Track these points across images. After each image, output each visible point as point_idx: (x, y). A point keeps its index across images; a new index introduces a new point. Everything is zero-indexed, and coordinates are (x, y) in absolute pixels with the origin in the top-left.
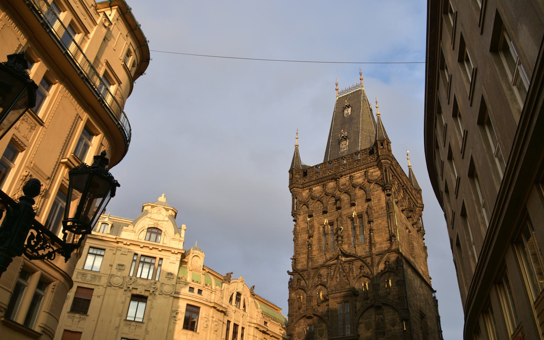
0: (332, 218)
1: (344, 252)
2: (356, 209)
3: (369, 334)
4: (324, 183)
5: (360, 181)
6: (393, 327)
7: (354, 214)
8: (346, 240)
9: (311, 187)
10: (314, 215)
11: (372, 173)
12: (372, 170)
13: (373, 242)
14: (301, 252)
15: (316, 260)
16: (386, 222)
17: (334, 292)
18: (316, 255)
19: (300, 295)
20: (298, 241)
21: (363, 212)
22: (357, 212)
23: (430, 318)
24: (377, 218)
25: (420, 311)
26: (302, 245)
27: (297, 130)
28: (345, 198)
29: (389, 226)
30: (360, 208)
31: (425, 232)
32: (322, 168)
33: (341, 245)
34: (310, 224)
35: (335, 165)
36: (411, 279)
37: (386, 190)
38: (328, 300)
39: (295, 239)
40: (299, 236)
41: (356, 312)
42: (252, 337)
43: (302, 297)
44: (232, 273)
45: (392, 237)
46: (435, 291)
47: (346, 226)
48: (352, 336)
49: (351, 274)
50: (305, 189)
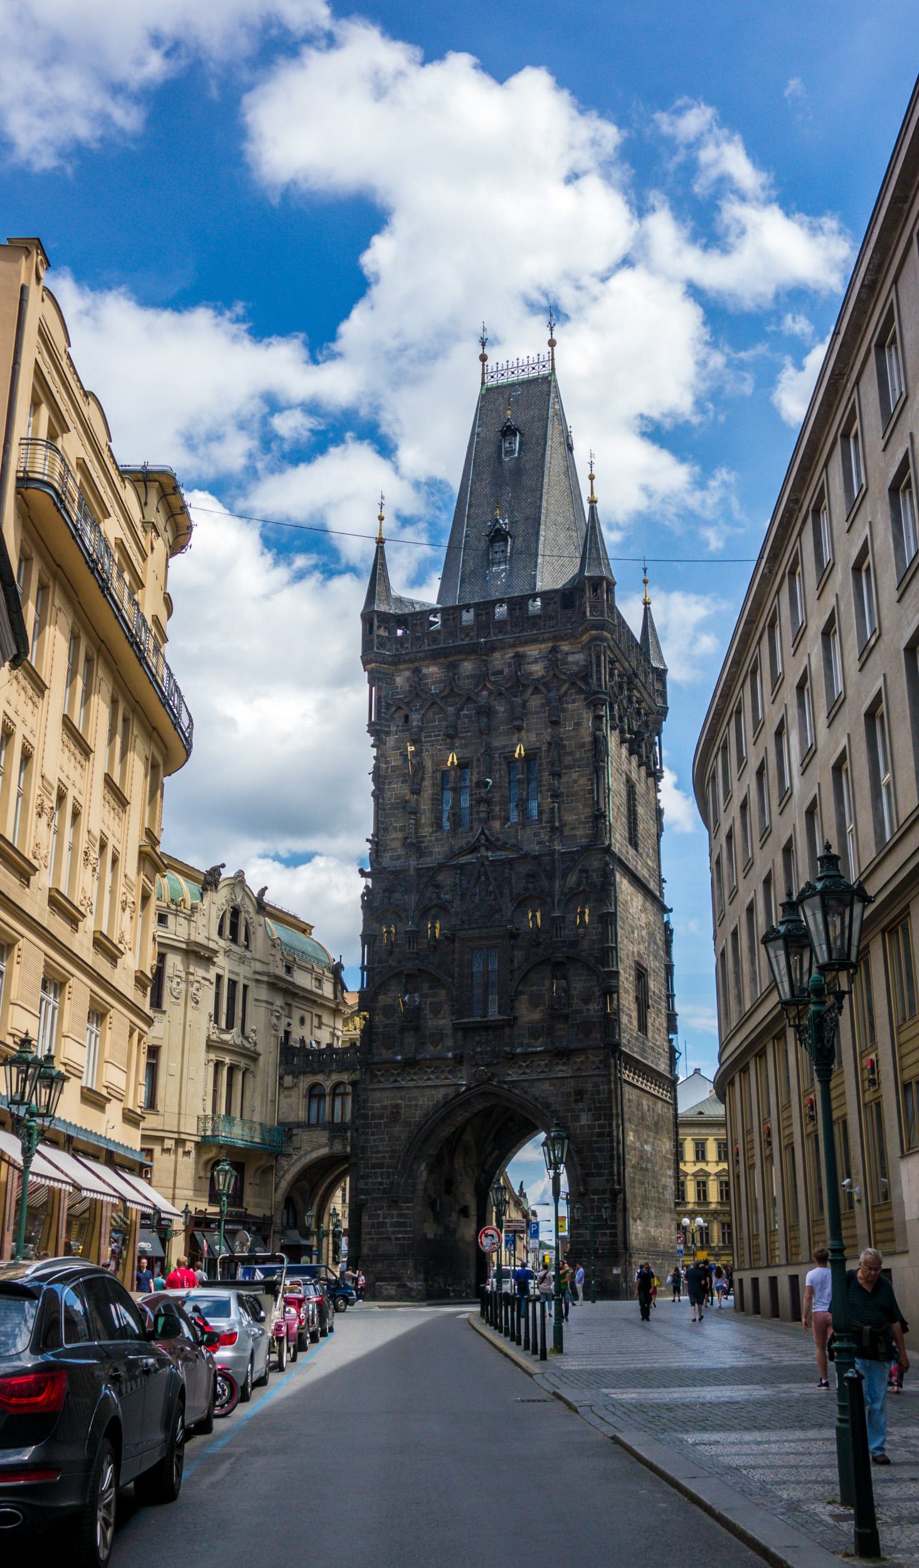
0: (467, 753)
1: (493, 839)
3: (537, 1016)
4: (451, 659)
5: (537, 669)
6: (587, 1004)
8: (497, 809)
9: (417, 664)
10: (423, 739)
11: (567, 654)
12: (565, 647)
13: (557, 824)
15: (426, 848)
16: (589, 780)
17: (466, 927)
18: (425, 836)
19: (390, 927)
20: (383, 799)
21: (540, 748)
23: (654, 971)
25: (638, 964)
27: (382, 497)
28: (501, 708)
29: (592, 790)
30: (533, 737)
31: (664, 774)
32: (448, 619)
33: (486, 821)
35: (480, 617)
36: (626, 902)
37: (595, 706)
38: (454, 940)
39: (377, 793)
41: (511, 972)
42: (264, 1005)
44: (223, 866)
45: (599, 817)
46: (671, 910)
48: (503, 1020)
49: (506, 891)
50: (402, 667)
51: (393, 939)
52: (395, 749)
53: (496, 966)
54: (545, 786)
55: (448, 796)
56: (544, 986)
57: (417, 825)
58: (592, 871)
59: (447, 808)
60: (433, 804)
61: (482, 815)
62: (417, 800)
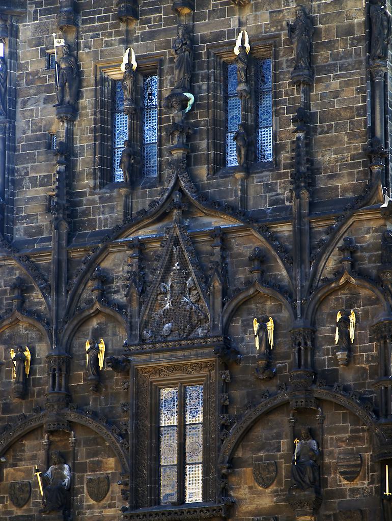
0: (153, 48)
2: (251, 24)
3: (266, 500)
7: (239, 43)
8: (203, 144)
14: (27, 174)
15: (85, 213)
16: (360, 91)
18: (84, 193)
22: (252, 33)
24: (328, 69)
26: (30, 147)
30: (264, 18)
34: (63, 66)
40: (19, 109)
43: (27, 354)
47: (205, 87)
51: (28, 371)
52: (30, 42)
53: (200, 418)
54: (285, 102)
55: (123, 123)
56: (279, 450)
57: (68, 178)
58: (363, 249)
59: (121, 142)
60: (95, 141)
61: (177, 154)
62: (70, 134)
